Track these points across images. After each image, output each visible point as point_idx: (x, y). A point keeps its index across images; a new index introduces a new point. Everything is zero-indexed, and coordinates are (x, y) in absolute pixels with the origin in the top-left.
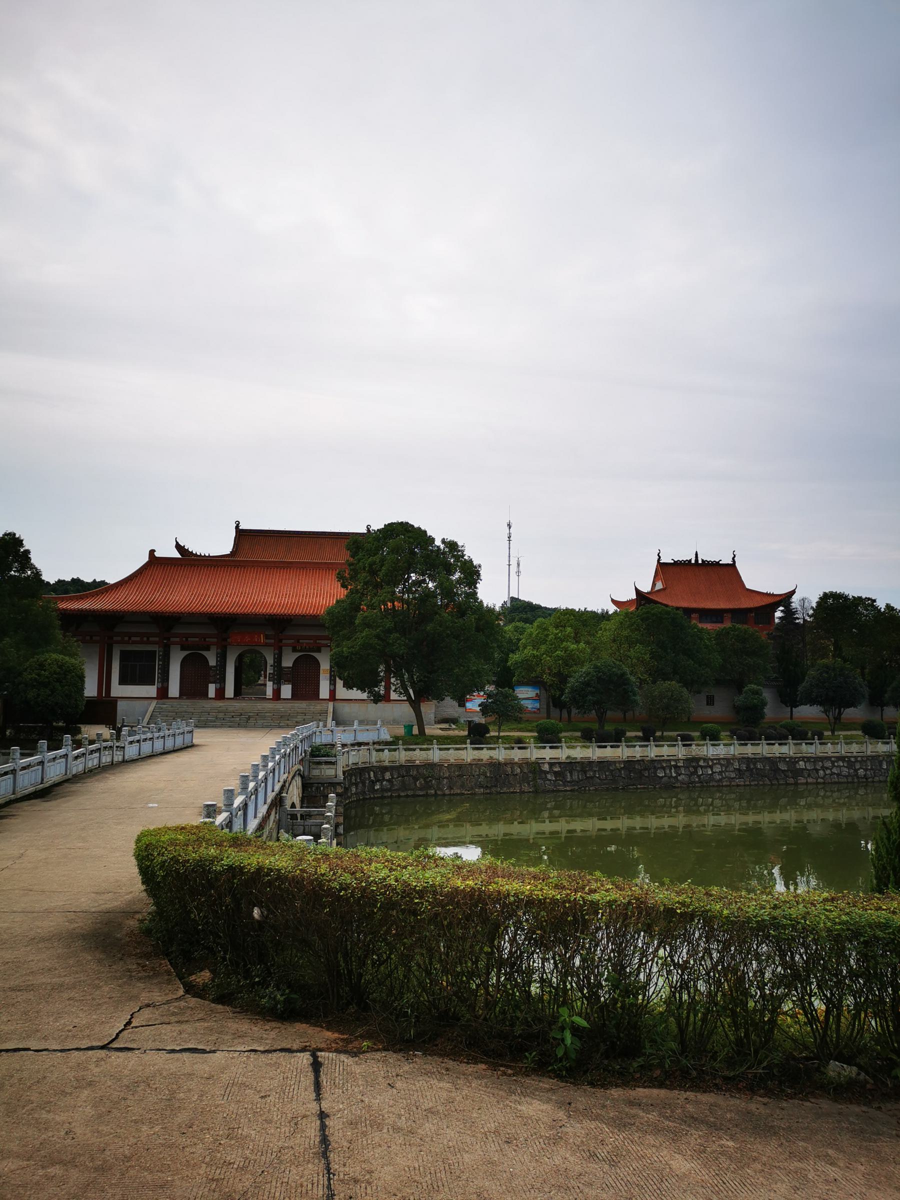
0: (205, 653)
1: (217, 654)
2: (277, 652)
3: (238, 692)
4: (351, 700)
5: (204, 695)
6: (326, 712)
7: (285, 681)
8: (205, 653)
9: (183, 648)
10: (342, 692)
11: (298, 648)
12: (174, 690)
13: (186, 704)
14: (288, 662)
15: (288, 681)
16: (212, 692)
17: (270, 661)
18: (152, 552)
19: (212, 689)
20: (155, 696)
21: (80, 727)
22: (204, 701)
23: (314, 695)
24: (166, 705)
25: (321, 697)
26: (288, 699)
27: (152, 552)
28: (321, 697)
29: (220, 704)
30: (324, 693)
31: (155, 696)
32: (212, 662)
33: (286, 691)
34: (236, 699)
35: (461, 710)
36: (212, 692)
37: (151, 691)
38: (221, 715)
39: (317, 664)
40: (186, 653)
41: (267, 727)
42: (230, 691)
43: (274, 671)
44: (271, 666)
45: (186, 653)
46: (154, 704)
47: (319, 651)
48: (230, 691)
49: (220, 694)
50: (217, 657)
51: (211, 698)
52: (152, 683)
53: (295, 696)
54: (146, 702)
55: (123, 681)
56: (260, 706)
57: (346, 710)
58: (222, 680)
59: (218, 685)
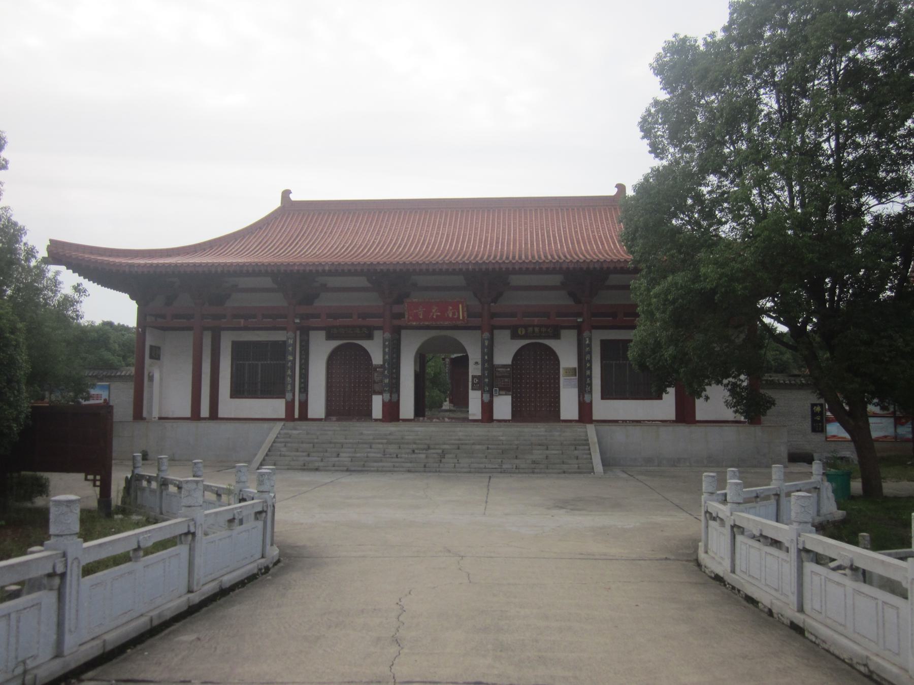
0: (365, 344)
1: (384, 340)
2: (486, 335)
3: (419, 411)
4: (616, 421)
5: (365, 413)
6: (586, 442)
7: (501, 389)
8: (365, 344)
9: (330, 337)
10: (603, 409)
11: (521, 331)
12: (317, 406)
13: (336, 430)
14: (504, 356)
15: (505, 390)
16: (377, 410)
17: (475, 356)
18: (286, 194)
19: (377, 404)
20: (284, 417)
21: (47, 480)
22: (365, 424)
23: (552, 413)
24: (300, 430)
25: (562, 418)
26: (505, 421)
27: (286, 194)
28: (562, 418)
29: (391, 428)
30: (569, 407)
31: (284, 417)
32: (377, 359)
33: (503, 406)
34: (418, 421)
35: (818, 438)
36: (377, 410)
37: (275, 407)
38: (392, 449)
39: (554, 359)
40: (335, 343)
41: (479, 471)
42: (407, 407)
43: (483, 369)
44: (477, 363)
45: (335, 343)
46: (280, 425)
47: (556, 336)
48: (407, 407)
49: (392, 412)
50: (384, 346)
51: (376, 420)
52: (280, 394)
53: (519, 414)
54: (266, 425)
55: (237, 392)
56: (461, 431)
57: (618, 435)
58: (395, 387)
59: (387, 396)
